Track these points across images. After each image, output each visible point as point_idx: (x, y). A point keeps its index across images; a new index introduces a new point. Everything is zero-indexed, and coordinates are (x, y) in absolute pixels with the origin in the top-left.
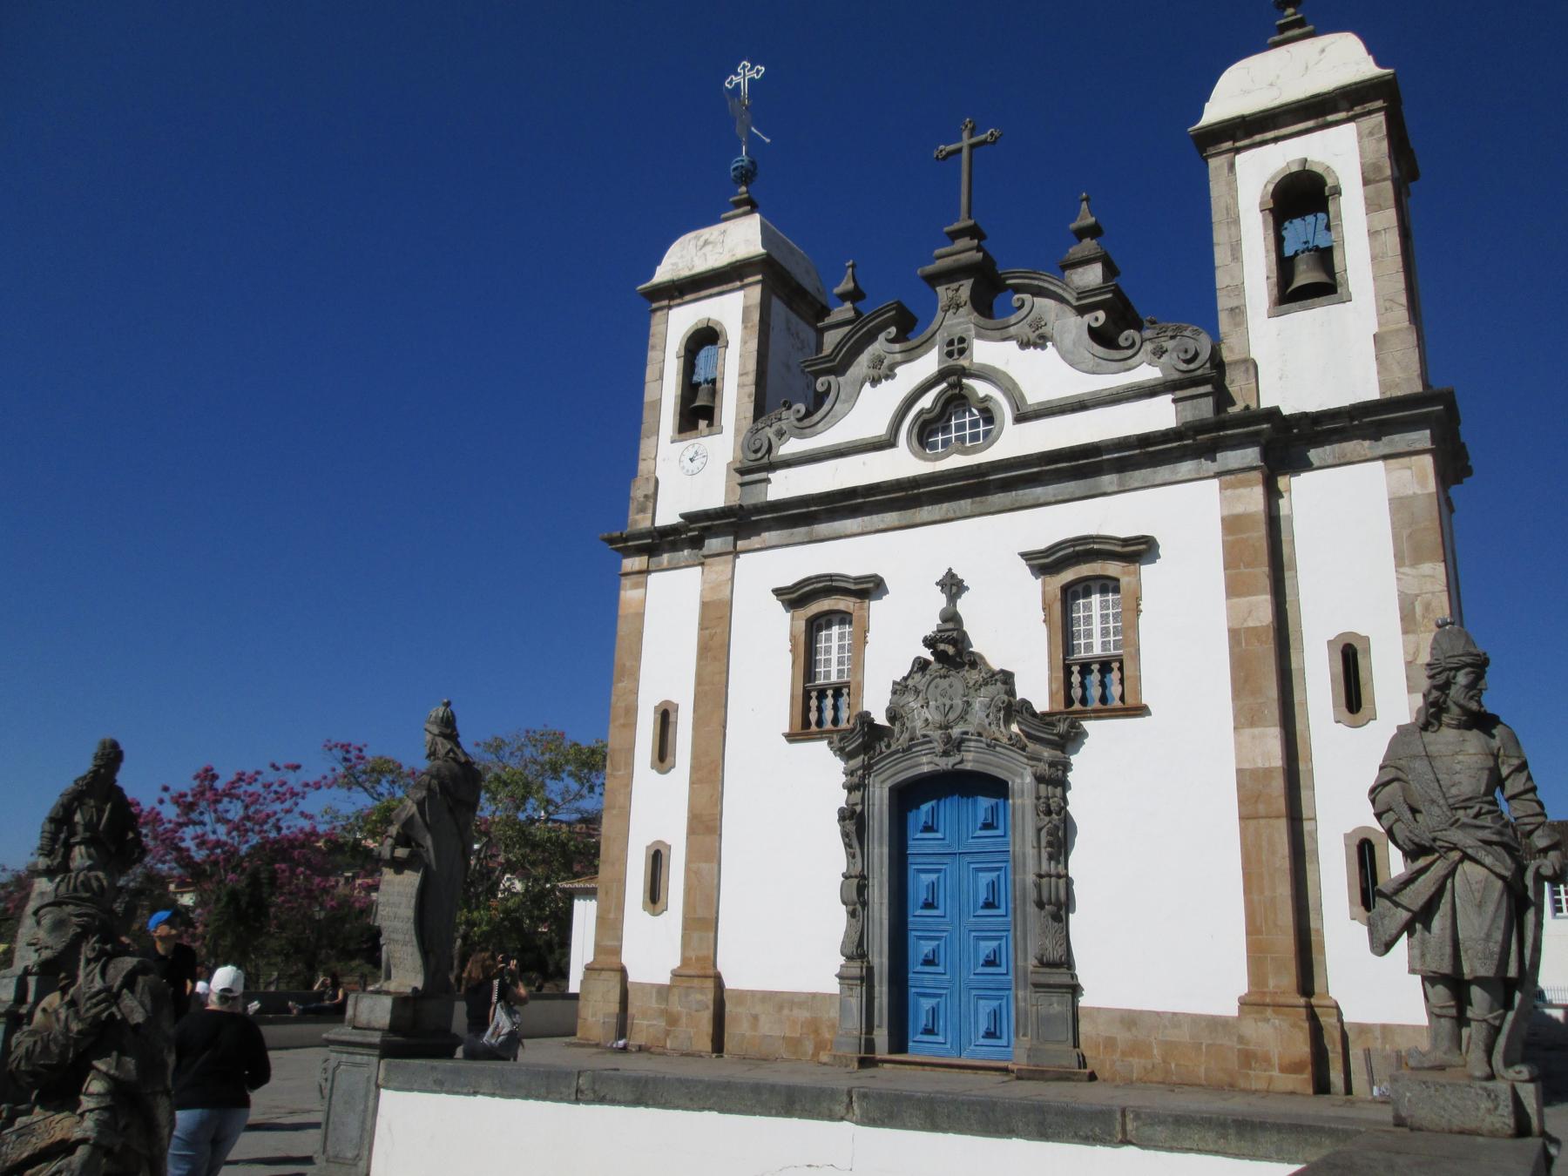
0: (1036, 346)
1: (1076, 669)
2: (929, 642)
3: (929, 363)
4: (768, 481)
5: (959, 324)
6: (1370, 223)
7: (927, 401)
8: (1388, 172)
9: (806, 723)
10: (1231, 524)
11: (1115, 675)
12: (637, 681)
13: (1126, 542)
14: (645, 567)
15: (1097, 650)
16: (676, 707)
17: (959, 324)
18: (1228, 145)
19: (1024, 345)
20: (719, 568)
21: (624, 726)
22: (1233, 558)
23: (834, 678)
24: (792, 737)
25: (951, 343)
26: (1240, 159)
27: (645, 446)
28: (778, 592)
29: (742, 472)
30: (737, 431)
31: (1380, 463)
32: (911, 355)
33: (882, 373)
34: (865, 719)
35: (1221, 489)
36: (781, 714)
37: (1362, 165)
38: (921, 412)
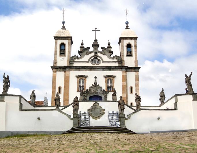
0: (104, 55)
2: (94, 83)
9: (79, 90)
10: (123, 76)
11: (112, 88)
13: (114, 76)
14: (56, 70)
15: (110, 86)
16: (61, 87)
18: (123, 39)
19: (103, 55)
22: (123, 79)
23: (82, 86)
24: (77, 91)
25: (95, 53)
26: (124, 41)
28: (76, 76)
29: (70, 62)
30: (68, 57)
32: (91, 52)
34: (87, 90)
35: (122, 72)
36: (76, 89)
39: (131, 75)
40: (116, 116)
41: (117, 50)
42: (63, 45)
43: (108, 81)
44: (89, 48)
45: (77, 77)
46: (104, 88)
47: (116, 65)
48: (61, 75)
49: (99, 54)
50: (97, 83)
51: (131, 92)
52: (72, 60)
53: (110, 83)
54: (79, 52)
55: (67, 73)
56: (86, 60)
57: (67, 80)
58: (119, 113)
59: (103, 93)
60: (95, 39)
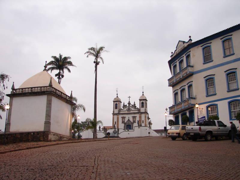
10: (139, 116)
20: (118, 116)
22: (139, 117)
39: (143, 116)
41: (138, 106)
42: (116, 104)
44: (126, 105)
45: (122, 117)
46: (132, 122)
47: (137, 112)
48: (116, 117)
49: (130, 108)
51: (143, 122)
52: (119, 111)
54: (123, 107)
56: (125, 110)
59: (132, 124)
60: (129, 101)
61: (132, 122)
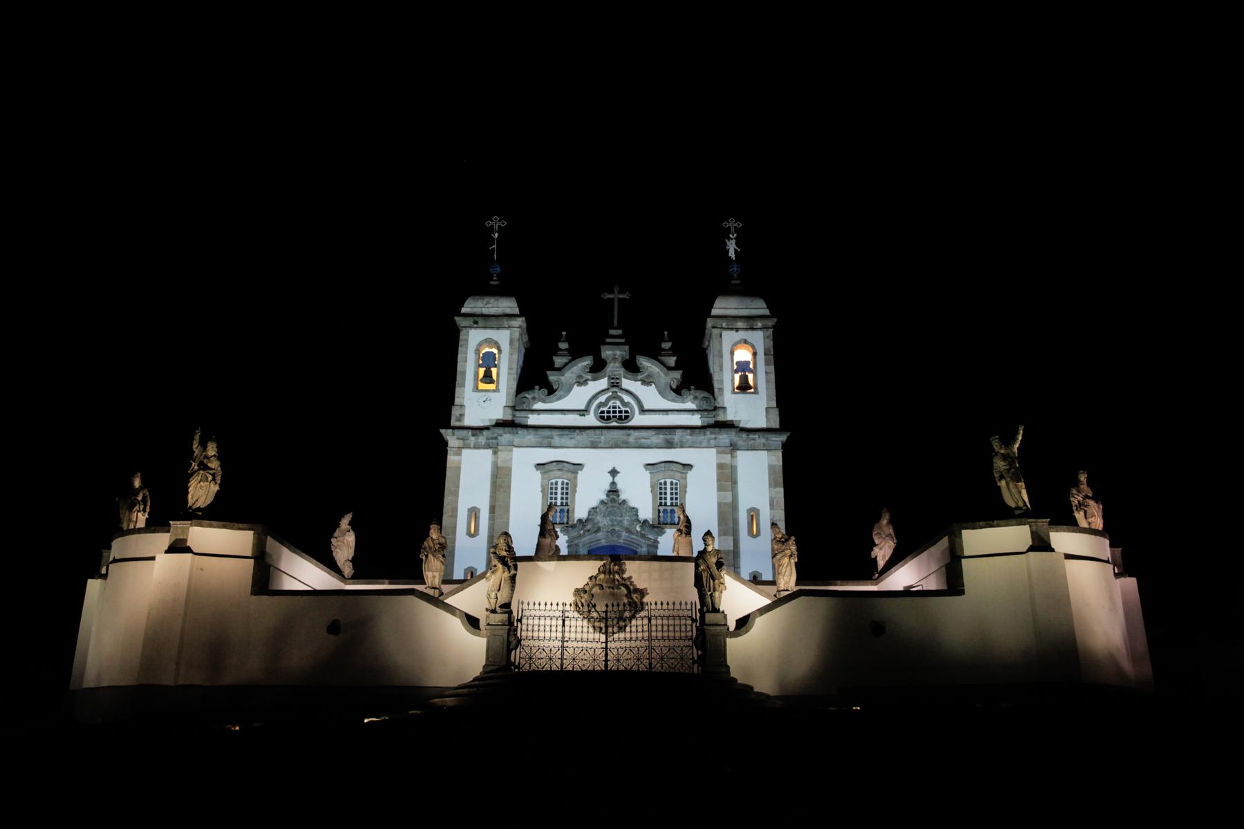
1: (661, 511)
3: (603, 383)
4: (528, 417)
5: (616, 371)
6: (766, 369)
7: (602, 399)
8: (772, 353)
10: (720, 466)
12: (458, 497)
16: (479, 510)
17: (616, 371)
21: (451, 516)
27: (458, 390)
30: (508, 394)
31: (766, 452)
33: (582, 382)
34: (580, 521)
37: (765, 349)
38: (601, 402)
40: (683, 622)
43: (661, 488)
46: (646, 512)
50: (618, 496)
53: (669, 496)
55: (502, 455)
57: (500, 482)
58: (698, 607)
61: (646, 512)
